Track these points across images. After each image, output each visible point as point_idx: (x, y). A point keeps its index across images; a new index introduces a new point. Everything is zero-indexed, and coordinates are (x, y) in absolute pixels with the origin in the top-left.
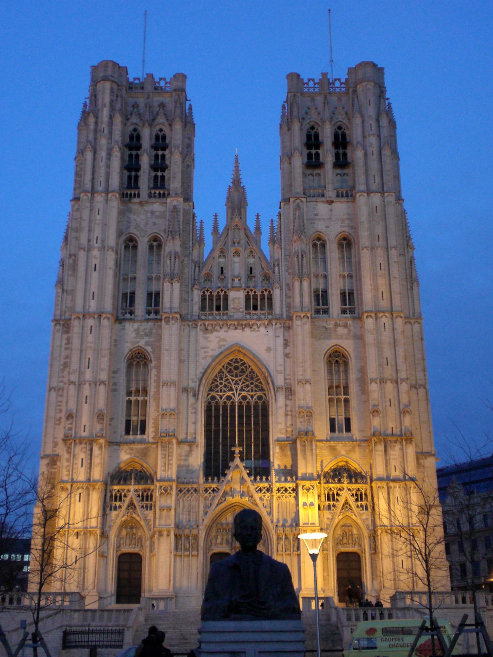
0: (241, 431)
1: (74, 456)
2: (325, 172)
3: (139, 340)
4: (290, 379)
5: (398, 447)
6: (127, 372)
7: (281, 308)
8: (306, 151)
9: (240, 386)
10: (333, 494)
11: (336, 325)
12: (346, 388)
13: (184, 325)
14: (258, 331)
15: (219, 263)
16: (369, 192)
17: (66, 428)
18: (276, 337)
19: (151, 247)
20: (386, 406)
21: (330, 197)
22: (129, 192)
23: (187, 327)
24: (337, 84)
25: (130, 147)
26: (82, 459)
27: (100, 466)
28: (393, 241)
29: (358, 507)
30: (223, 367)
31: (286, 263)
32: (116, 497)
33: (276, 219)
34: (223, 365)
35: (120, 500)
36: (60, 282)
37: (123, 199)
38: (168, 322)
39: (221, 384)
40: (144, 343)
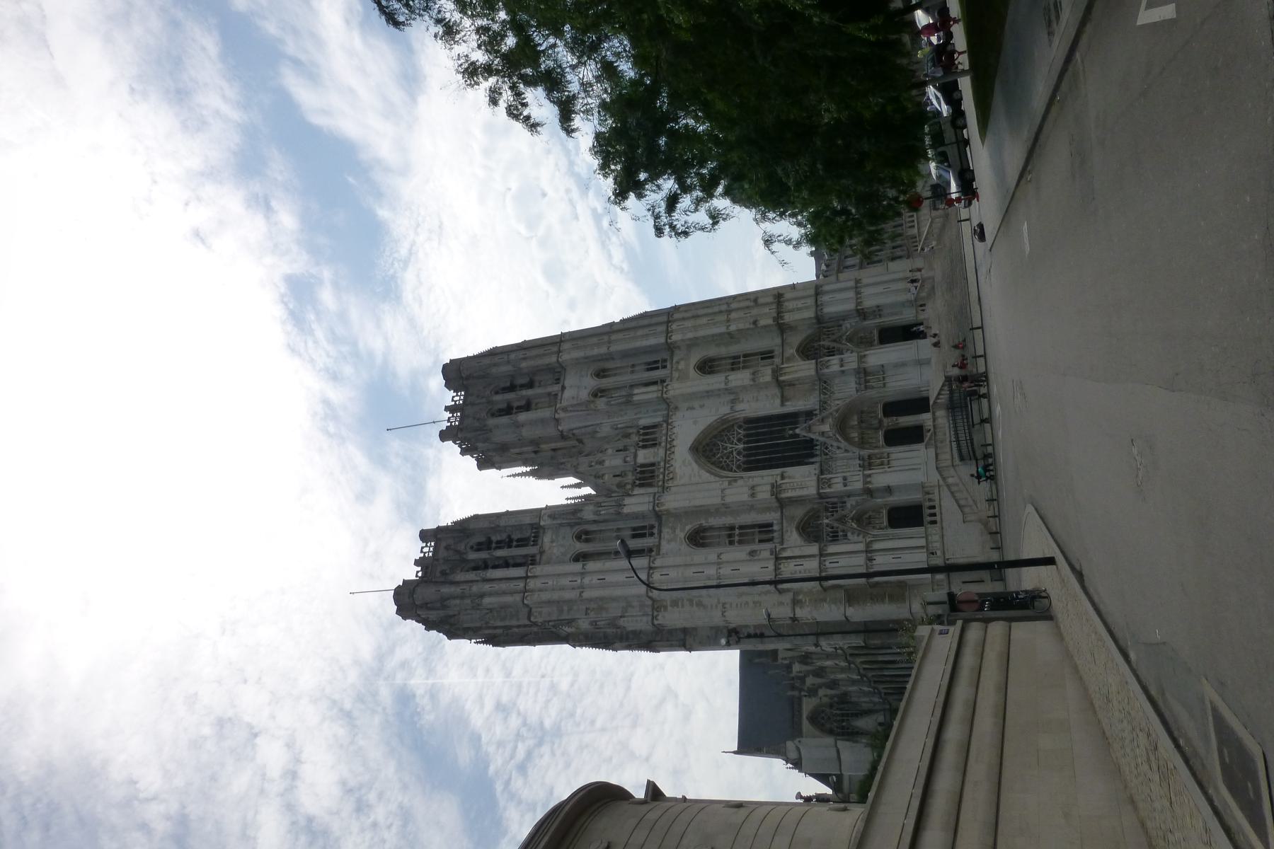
0: (771, 439)
3: (678, 539)
5: (786, 304)
11: (677, 369)
14: (677, 433)
16: (559, 351)
19: (587, 541)
30: (709, 461)
32: (833, 536)
38: (662, 504)
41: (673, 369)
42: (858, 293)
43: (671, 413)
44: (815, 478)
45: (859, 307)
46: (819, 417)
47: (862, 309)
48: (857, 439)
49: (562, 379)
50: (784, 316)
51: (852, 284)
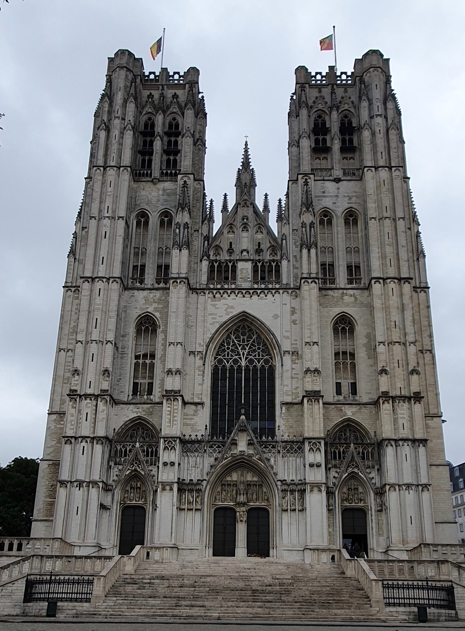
0: (247, 393)
1: (79, 411)
2: (332, 155)
3: (147, 306)
4: (297, 344)
6: (136, 337)
7: (288, 277)
8: (313, 138)
9: (247, 351)
10: (339, 453)
11: (343, 293)
12: (352, 355)
13: (192, 293)
15: (228, 238)
17: (72, 384)
18: (283, 304)
19: (162, 223)
20: (394, 367)
21: (337, 176)
22: (142, 172)
23: (196, 295)
24: (344, 77)
25: (144, 134)
26: (87, 413)
27: (105, 421)
28: (400, 214)
29: (364, 465)
31: (294, 237)
33: (284, 198)
34: (230, 331)
35: (125, 455)
36: (73, 252)
37: (136, 178)
39: (228, 348)
40: (153, 310)
41: (345, 291)
42: (408, 486)
43: (290, 291)
44: (179, 434)
45: (387, 487)
46: (255, 440)
47: (386, 492)
48: (229, 479)
49: (349, 178)
50: (388, 403)
51: (424, 481)
